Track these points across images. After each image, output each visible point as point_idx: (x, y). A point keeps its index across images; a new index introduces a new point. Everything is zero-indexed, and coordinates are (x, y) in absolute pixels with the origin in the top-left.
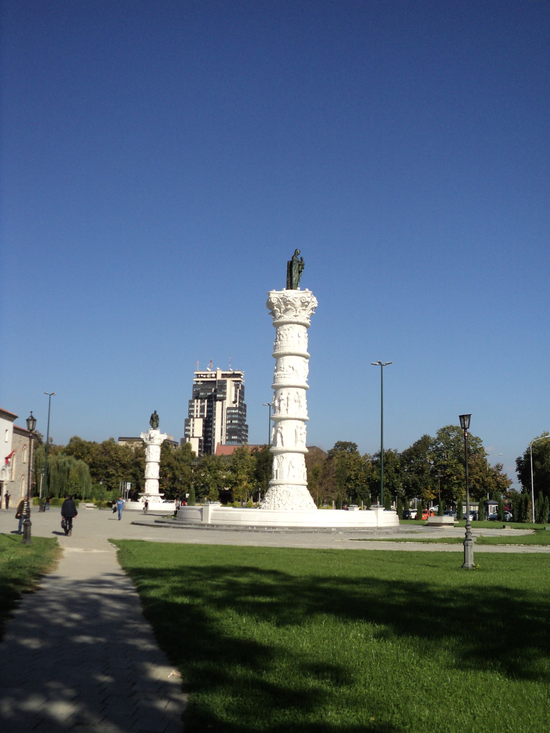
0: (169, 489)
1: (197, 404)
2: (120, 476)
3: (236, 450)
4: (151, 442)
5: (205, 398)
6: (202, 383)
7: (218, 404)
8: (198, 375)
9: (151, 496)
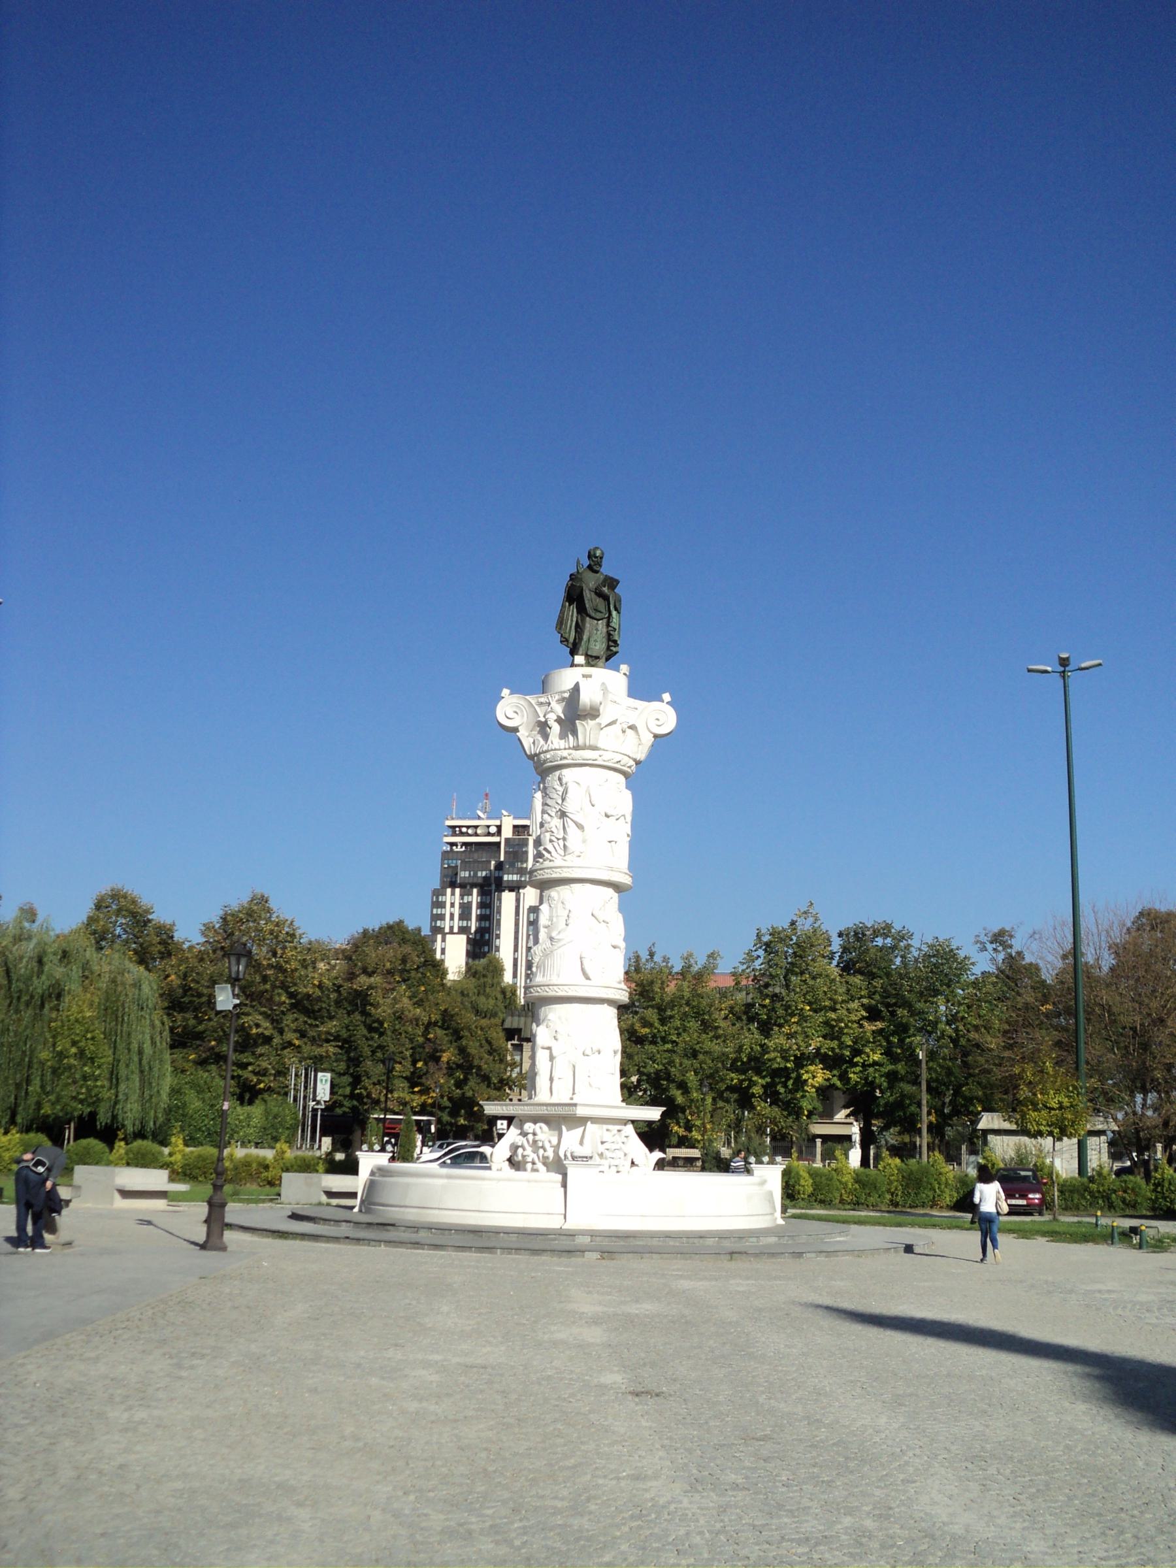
0: (445, 1102)
1: (453, 898)
2: (290, 1044)
3: (766, 938)
4: (577, 748)
5: (473, 885)
6: (464, 849)
7: (508, 898)
8: (454, 827)
9: (582, 1121)
